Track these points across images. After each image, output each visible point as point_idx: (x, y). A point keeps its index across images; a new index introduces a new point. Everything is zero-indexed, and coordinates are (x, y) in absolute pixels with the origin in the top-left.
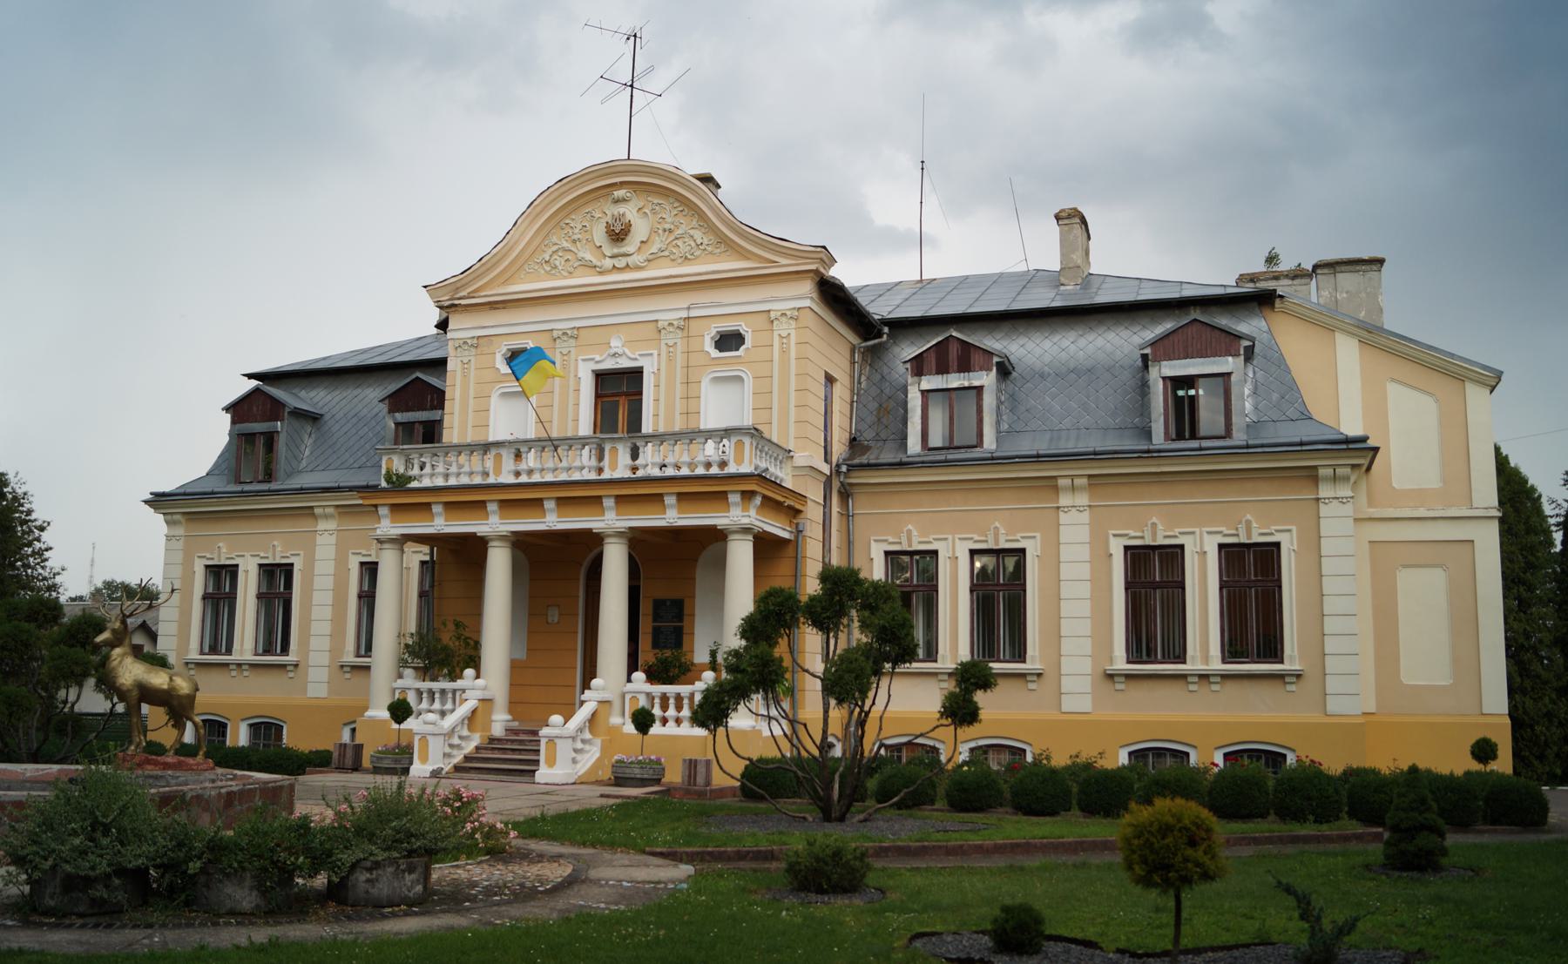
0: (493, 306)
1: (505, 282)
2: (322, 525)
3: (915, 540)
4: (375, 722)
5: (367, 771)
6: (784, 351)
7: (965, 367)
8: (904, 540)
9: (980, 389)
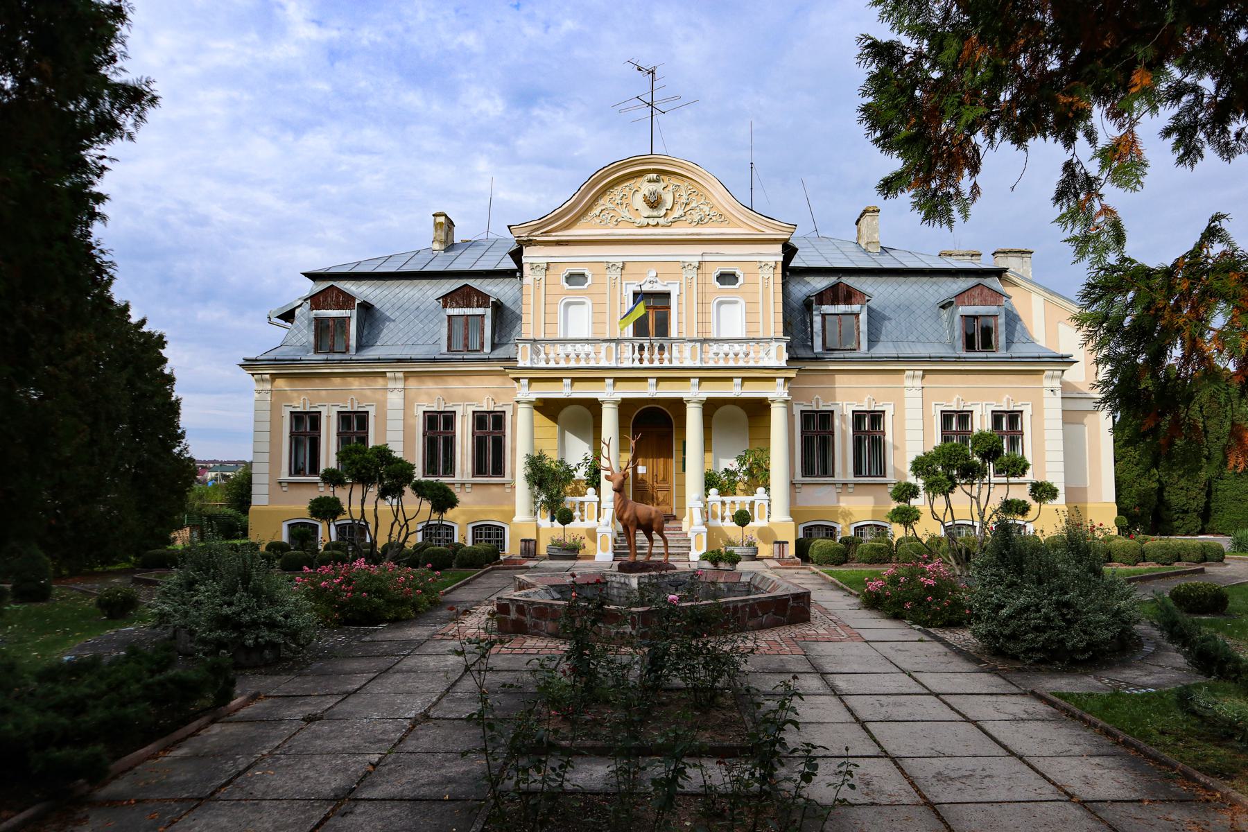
1: (567, 226)
2: (391, 385)
3: (821, 404)
5: (545, 558)
9: (857, 315)
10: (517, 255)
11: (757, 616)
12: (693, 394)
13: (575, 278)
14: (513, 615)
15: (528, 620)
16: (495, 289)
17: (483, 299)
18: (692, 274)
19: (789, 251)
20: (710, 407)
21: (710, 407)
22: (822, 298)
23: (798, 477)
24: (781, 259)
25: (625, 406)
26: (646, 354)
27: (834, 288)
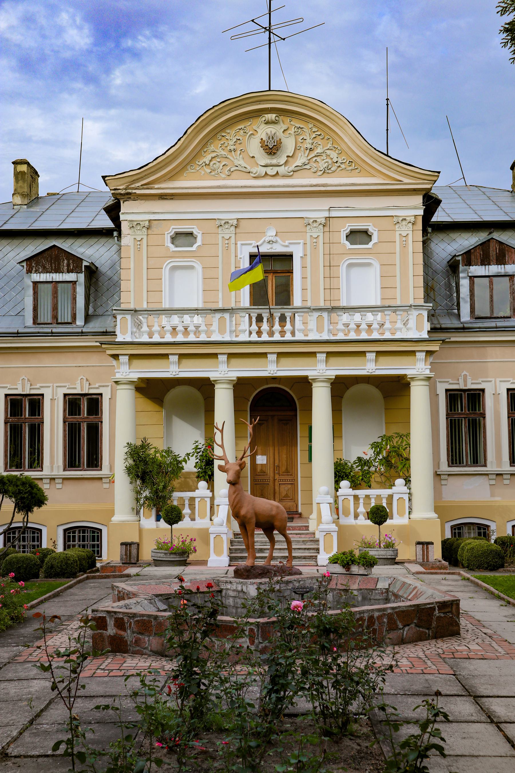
0: (162, 197)
1: (172, 176)
3: (469, 381)
4: (122, 524)
6: (404, 246)
7: (501, 260)
8: (461, 381)
10: (113, 211)
11: (397, 628)
12: (321, 371)
13: (184, 237)
14: (111, 630)
15: (128, 636)
16: (89, 251)
17: (75, 263)
18: (317, 232)
19: (431, 203)
20: (340, 387)
21: (340, 387)
22: (468, 257)
23: (444, 467)
24: (421, 212)
25: (241, 386)
26: (265, 326)
27: (484, 245)
